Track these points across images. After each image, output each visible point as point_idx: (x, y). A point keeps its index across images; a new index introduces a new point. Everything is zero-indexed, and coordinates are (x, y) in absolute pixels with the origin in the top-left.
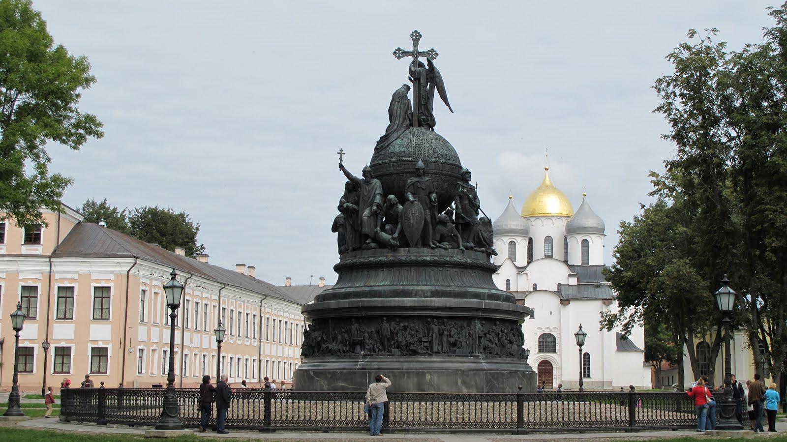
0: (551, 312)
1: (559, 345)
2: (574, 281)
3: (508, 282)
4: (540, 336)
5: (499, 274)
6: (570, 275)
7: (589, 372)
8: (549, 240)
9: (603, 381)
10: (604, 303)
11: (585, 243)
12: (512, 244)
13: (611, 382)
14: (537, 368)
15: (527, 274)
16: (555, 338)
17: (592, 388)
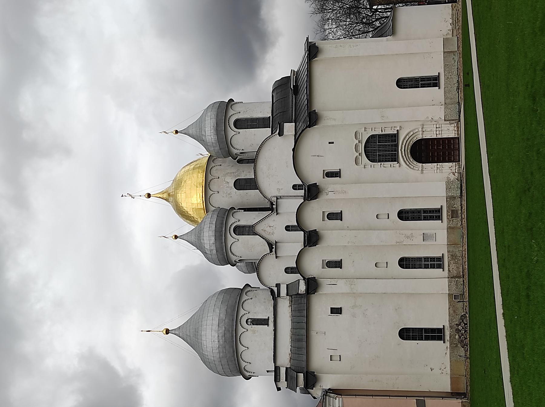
0: (330, 143)
1: (383, 131)
2: (289, 128)
3: (288, 228)
4: (369, 160)
5: (276, 242)
6: (281, 134)
7: (429, 78)
8: (240, 184)
9: (444, 52)
10: (315, 56)
11: (240, 124)
12: (240, 230)
13: (446, 41)
14: (424, 164)
15: (277, 199)
16: (373, 136)
17: (455, 72)
